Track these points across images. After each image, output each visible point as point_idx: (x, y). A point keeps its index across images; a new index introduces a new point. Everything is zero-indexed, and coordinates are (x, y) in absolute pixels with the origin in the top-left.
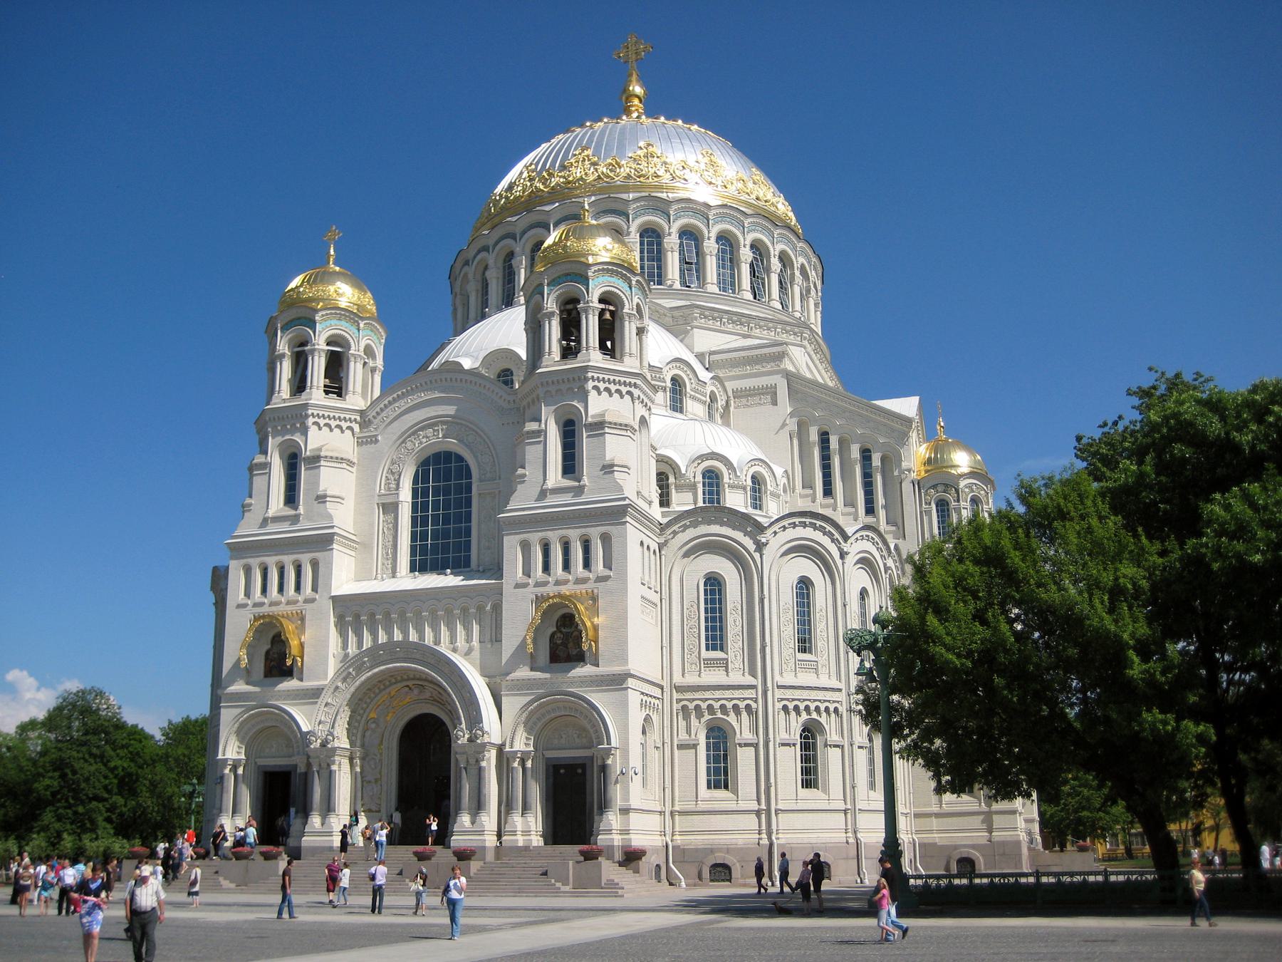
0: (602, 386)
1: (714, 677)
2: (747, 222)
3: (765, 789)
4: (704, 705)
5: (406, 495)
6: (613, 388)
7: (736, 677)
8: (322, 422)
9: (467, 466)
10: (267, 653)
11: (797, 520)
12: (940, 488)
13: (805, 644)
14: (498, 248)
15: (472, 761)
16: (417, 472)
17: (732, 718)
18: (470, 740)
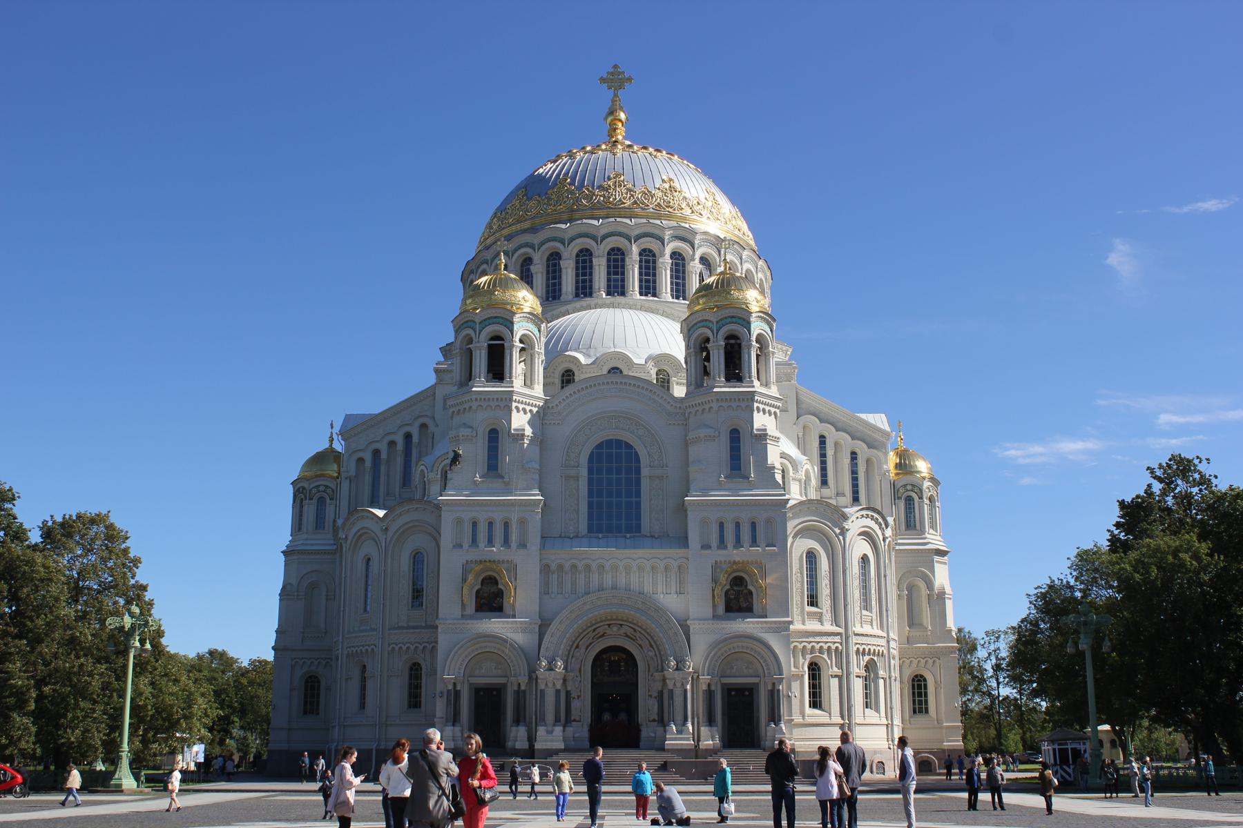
0: (761, 406)
1: (813, 626)
2: (745, 254)
3: (846, 709)
4: (809, 646)
5: (584, 472)
6: (767, 408)
7: (828, 627)
8: (521, 406)
9: (636, 453)
10: (478, 592)
11: (864, 513)
12: (909, 487)
13: (866, 605)
14: (544, 247)
15: (679, 685)
16: (592, 453)
17: (825, 656)
18: (677, 669)
